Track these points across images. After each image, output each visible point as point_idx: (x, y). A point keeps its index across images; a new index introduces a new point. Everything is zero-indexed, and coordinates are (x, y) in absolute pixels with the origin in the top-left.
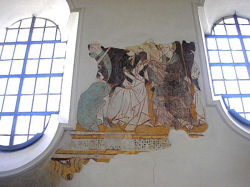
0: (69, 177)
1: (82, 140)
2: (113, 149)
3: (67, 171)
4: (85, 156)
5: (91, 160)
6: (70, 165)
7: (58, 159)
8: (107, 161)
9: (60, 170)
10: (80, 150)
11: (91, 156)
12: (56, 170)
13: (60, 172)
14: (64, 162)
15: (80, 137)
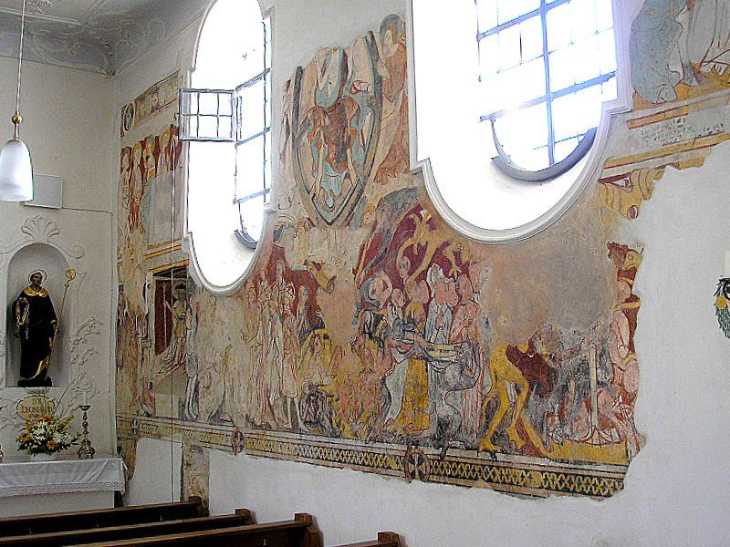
0: (633, 213)
1: (648, 128)
2: (710, 134)
3: (629, 199)
4: (656, 163)
5: (668, 166)
6: (632, 186)
7: (611, 180)
8: (698, 163)
9: (616, 200)
10: (647, 150)
11: (669, 159)
12: (609, 202)
13: (616, 206)
14: (620, 182)
15: (646, 122)
